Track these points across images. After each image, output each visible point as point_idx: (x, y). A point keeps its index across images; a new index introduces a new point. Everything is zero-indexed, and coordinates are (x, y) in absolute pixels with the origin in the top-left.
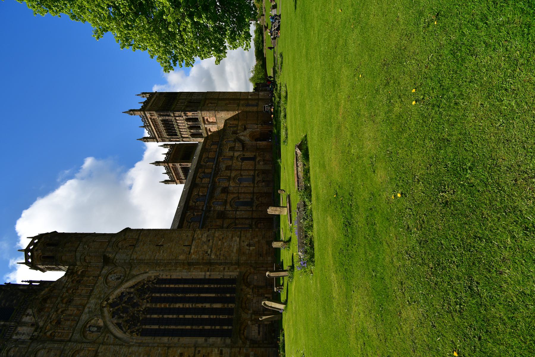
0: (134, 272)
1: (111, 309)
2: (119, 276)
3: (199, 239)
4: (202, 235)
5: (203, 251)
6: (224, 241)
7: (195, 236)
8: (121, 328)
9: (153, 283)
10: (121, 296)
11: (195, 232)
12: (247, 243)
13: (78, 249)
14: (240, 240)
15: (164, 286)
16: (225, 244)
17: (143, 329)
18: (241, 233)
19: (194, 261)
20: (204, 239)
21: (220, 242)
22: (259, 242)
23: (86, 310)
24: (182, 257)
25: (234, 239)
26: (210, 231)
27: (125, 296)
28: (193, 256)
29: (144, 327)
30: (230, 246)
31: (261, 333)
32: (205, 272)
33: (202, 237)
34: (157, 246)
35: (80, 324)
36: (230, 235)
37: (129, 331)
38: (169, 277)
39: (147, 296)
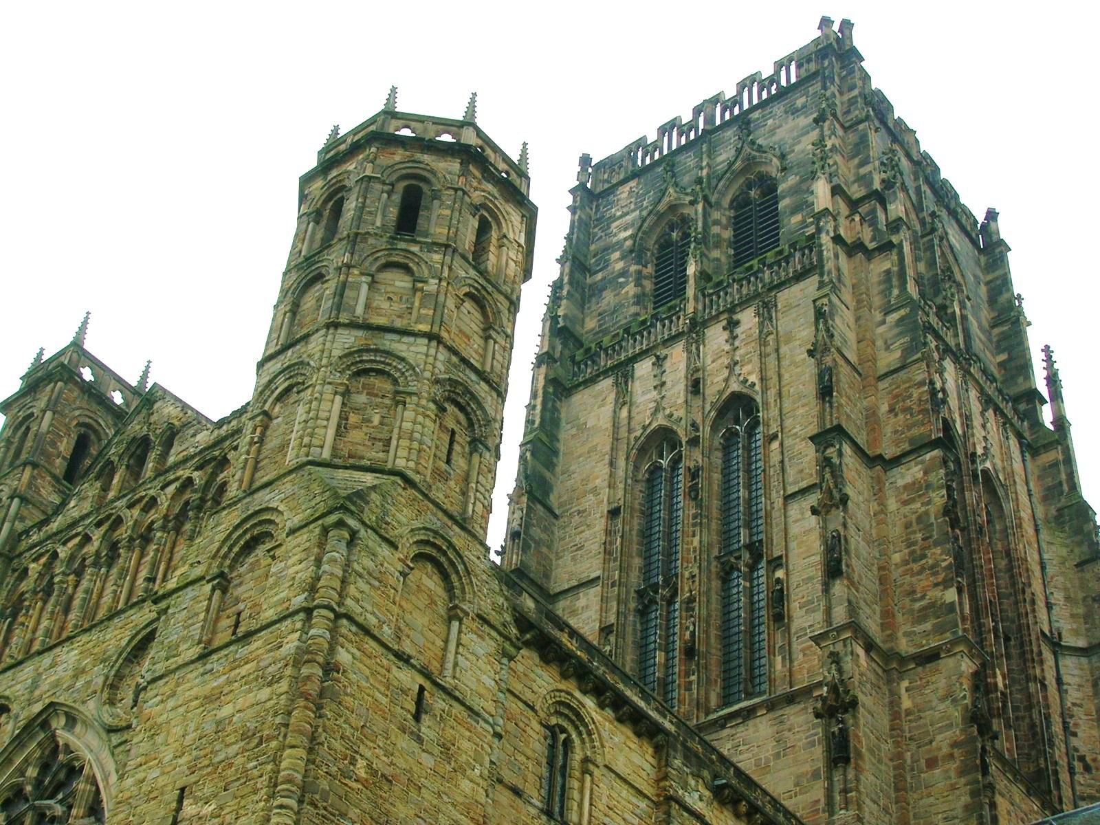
1: (32, 772)
10: (73, 771)
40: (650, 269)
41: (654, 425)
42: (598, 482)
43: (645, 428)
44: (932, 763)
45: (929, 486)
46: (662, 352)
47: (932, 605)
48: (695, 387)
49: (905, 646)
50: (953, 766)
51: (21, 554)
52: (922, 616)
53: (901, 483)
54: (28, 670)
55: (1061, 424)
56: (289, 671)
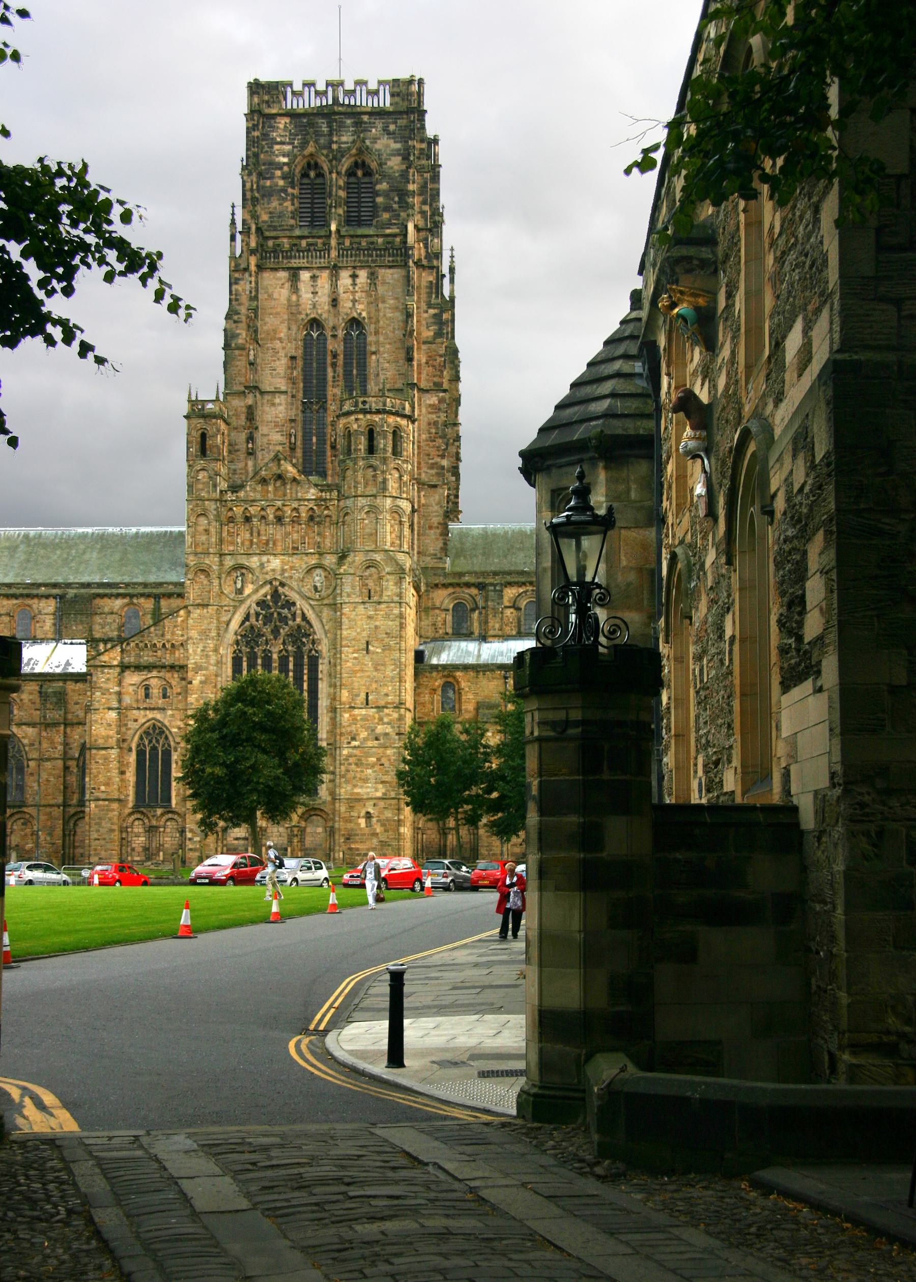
0: (326, 613)
1: (269, 597)
2: (319, 589)
3: (381, 719)
4: (388, 723)
5: (357, 730)
6: (377, 768)
7: (386, 711)
8: (243, 623)
9: (310, 651)
10: (290, 604)
11: (395, 707)
12: (372, 811)
13: (360, 498)
14: (379, 798)
15: (306, 671)
16: (369, 771)
17: (242, 658)
18: (393, 798)
19: (338, 719)
20: (380, 729)
21: (374, 759)
22: (375, 834)
23: (265, 559)
24: (345, 695)
25: (381, 786)
26: (397, 737)
27: (289, 609)
28: (346, 715)
29: (245, 659)
30: (365, 780)
31: (236, 842)
32: (327, 739)
33: (384, 724)
34: (368, 643)
35: (243, 561)
36: (387, 778)
37: (239, 638)
38: (320, 676)
39: (290, 648)
40: (296, 192)
41: (312, 316)
42: (282, 335)
43: (307, 315)
44: (430, 528)
45: (439, 409)
46: (317, 273)
47: (436, 463)
48: (335, 302)
49: (424, 477)
50: (438, 531)
51: (226, 501)
52: (432, 466)
53: (428, 402)
54: (255, 559)
55: (452, 299)
56: (398, 619)
